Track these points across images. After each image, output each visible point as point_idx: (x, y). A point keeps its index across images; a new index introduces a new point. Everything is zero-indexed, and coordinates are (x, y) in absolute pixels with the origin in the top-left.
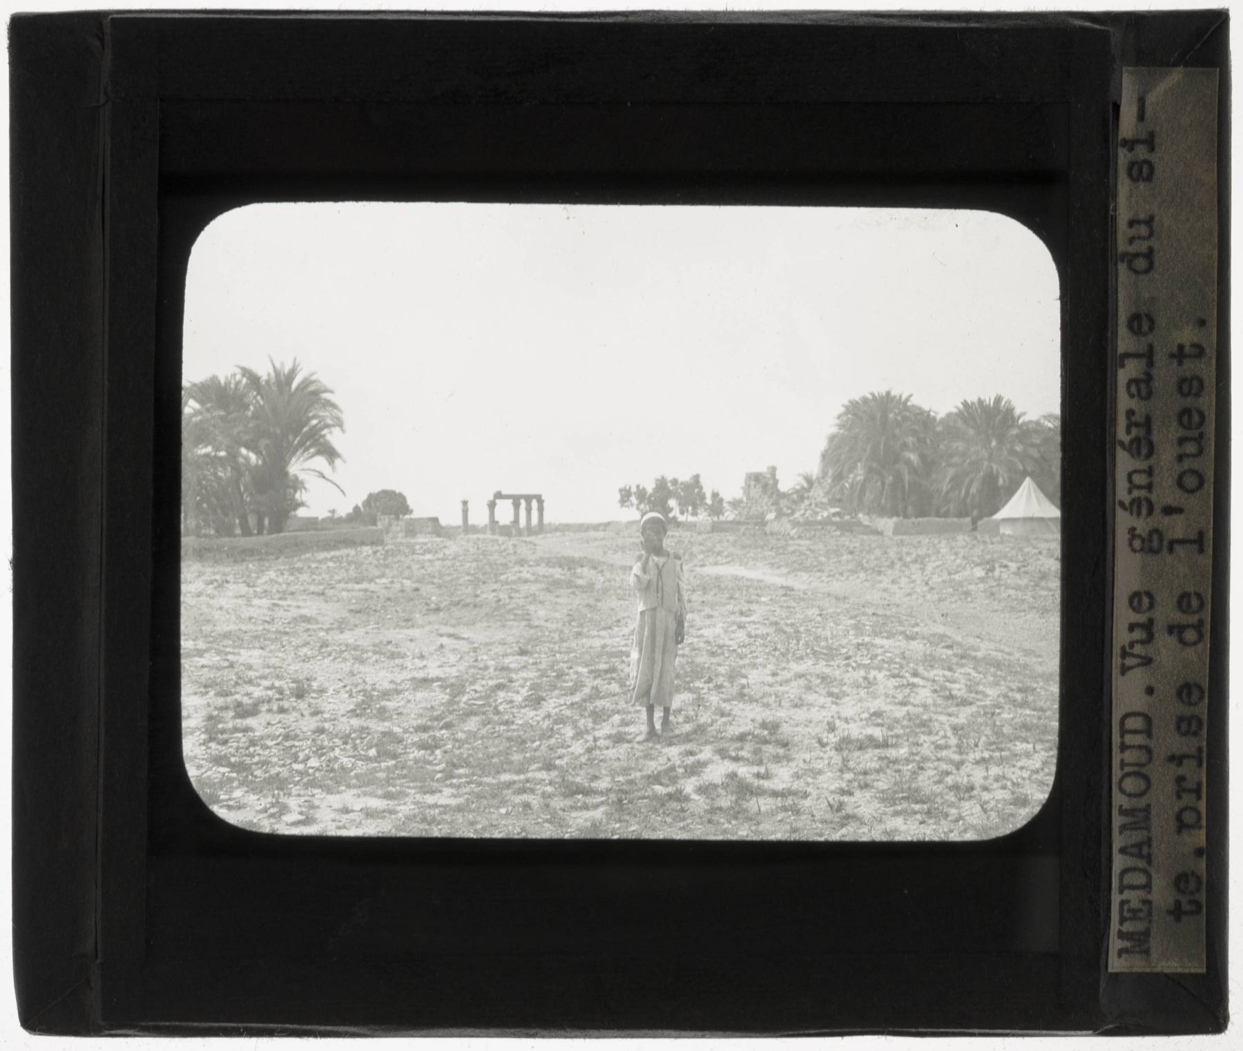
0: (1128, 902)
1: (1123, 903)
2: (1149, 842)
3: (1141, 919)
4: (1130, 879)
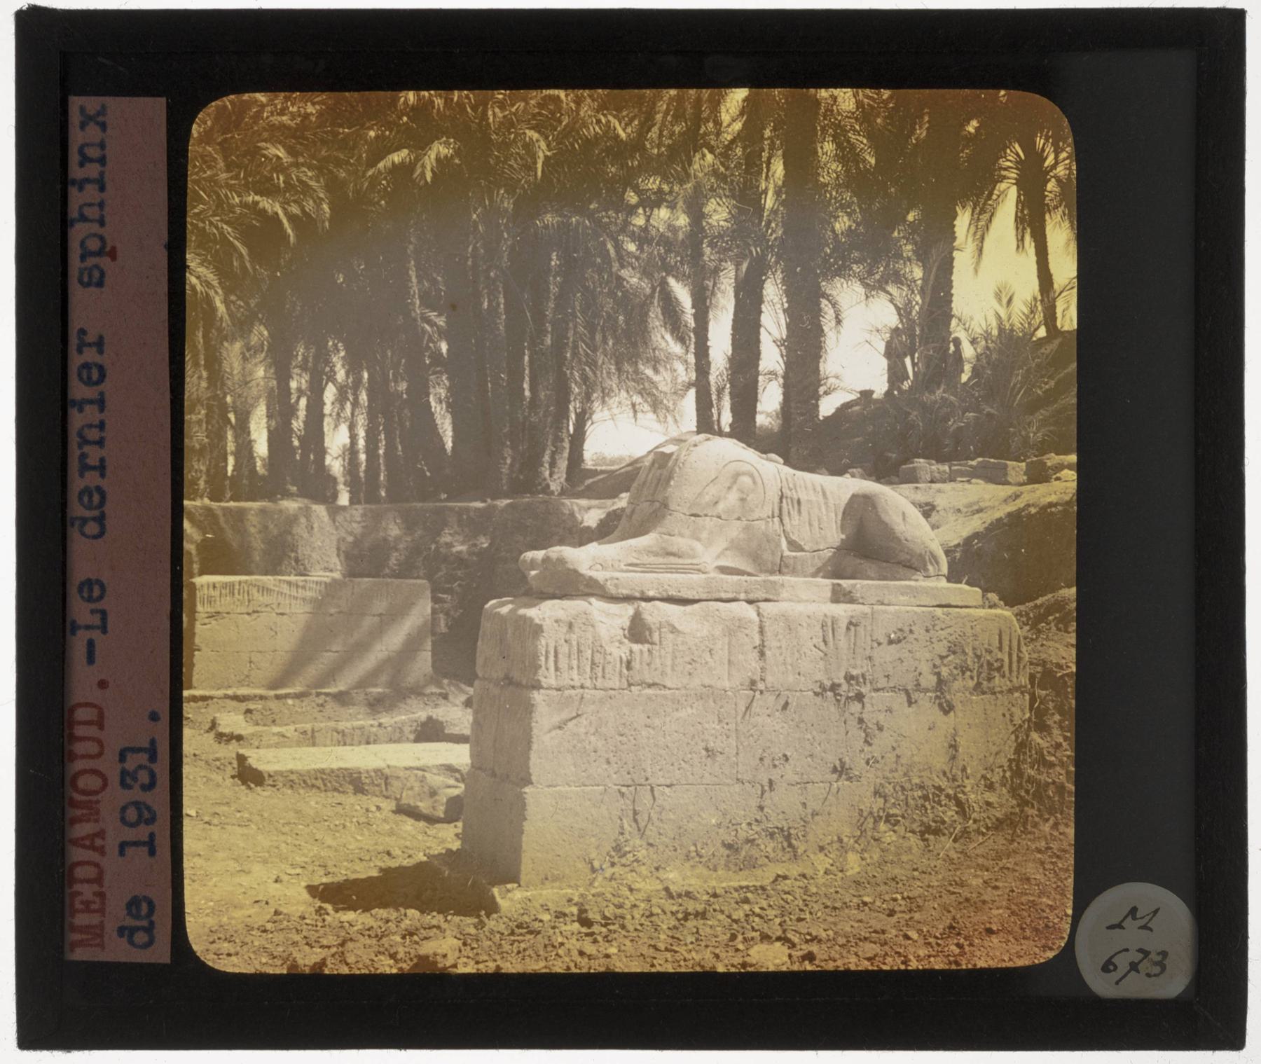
0: (79, 893)
3: (95, 911)
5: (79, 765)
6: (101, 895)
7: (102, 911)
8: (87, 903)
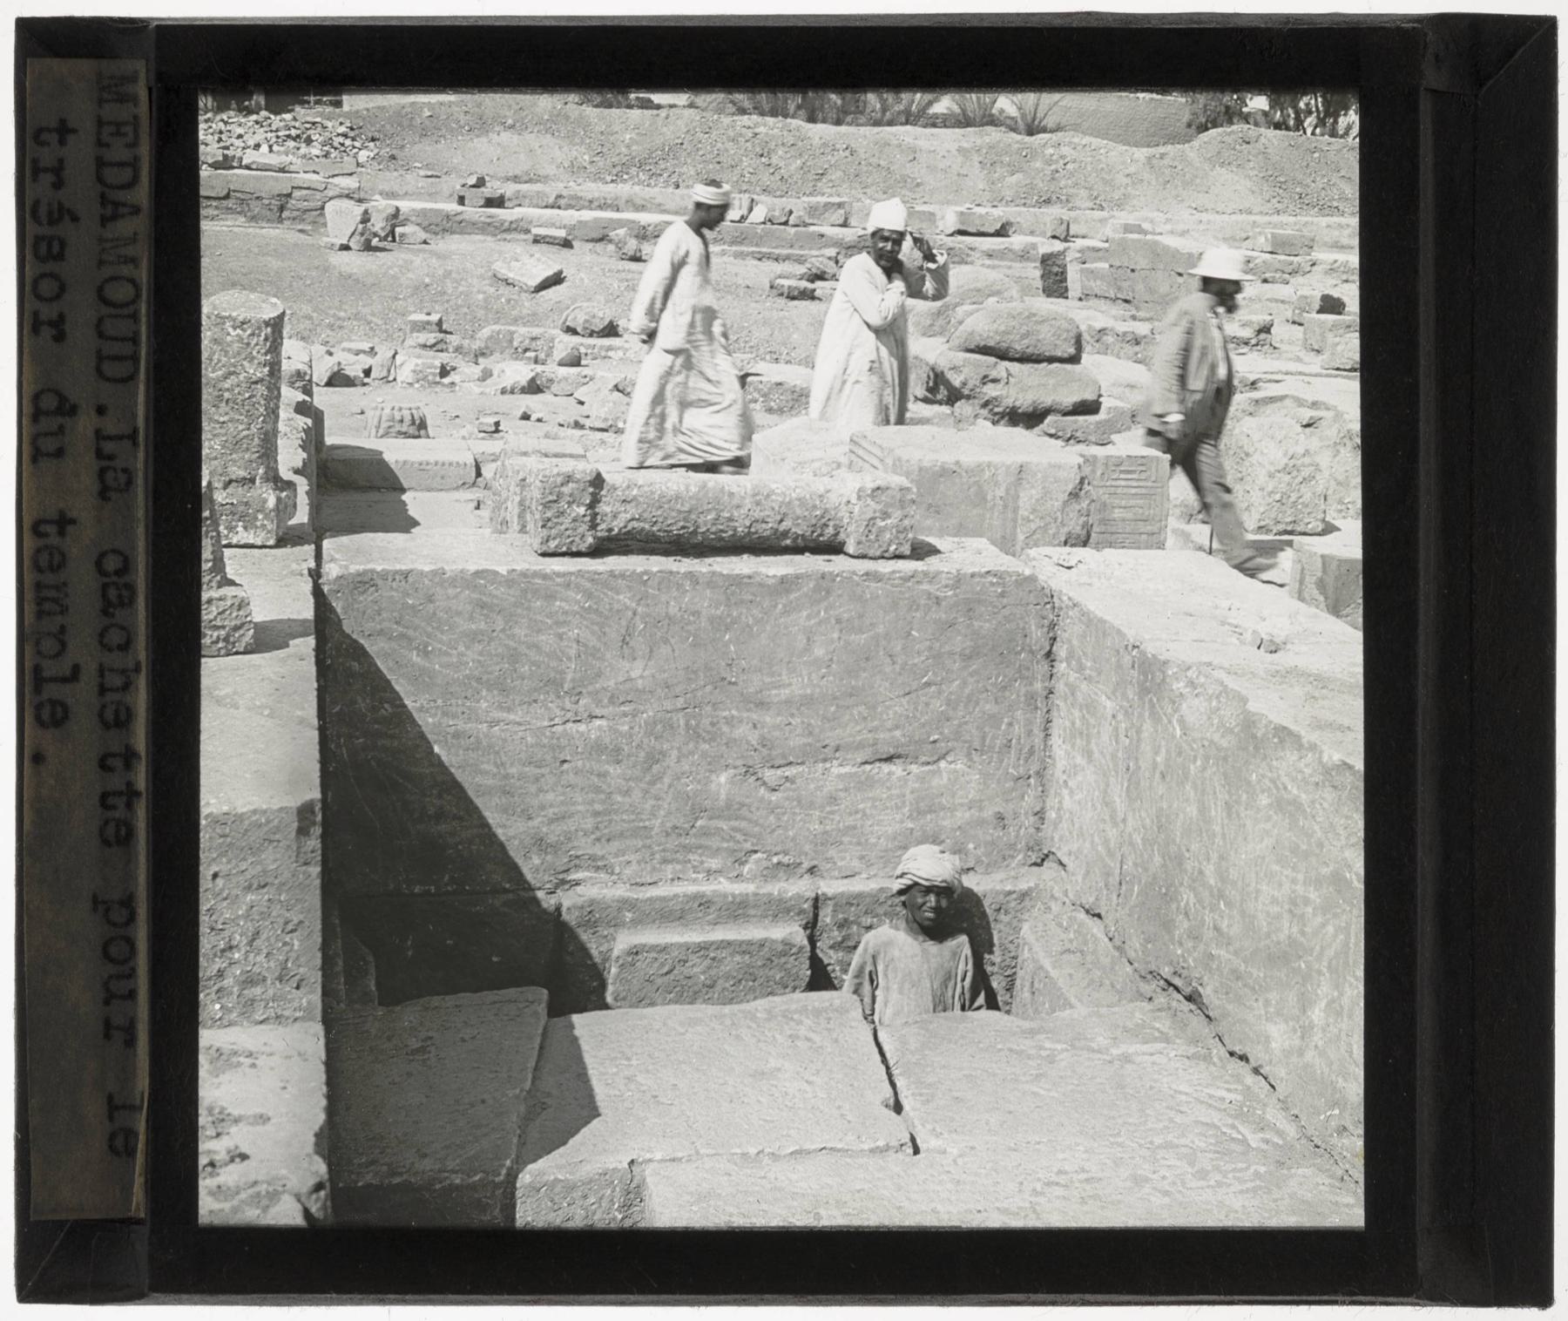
0: (129, 146)
1: (134, 144)
2: (104, 221)
4: (127, 174)
5: (125, 311)
6: (100, 143)
7: (100, 123)
8: (118, 134)
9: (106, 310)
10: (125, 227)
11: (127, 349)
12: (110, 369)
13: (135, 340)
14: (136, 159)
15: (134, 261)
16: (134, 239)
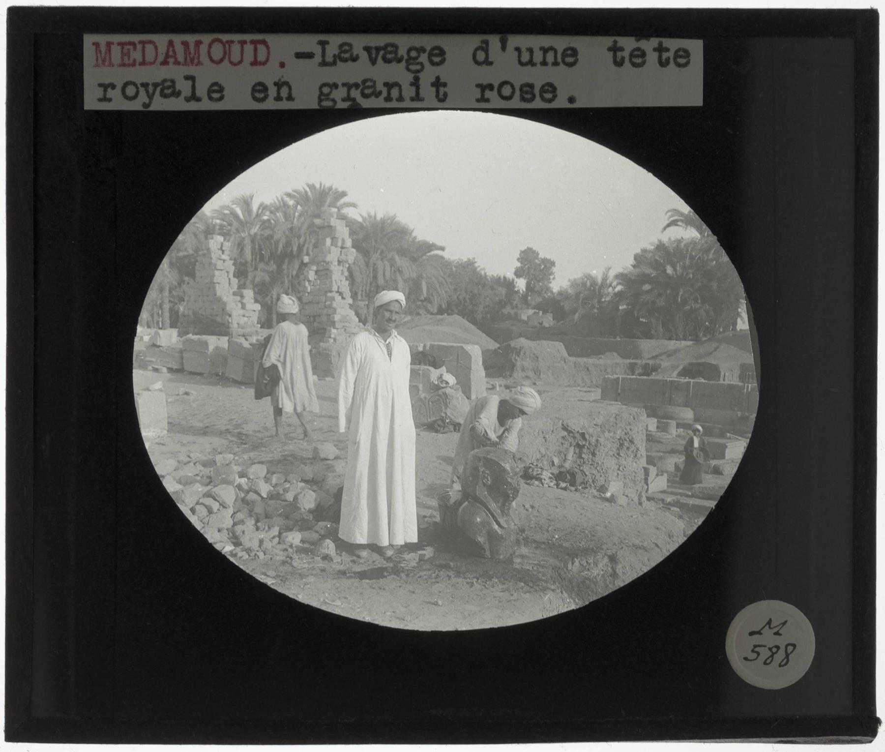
0: (135, 49)
1: (133, 44)
3: (122, 58)
4: (149, 48)
6: (134, 65)
7: (123, 65)
9: (226, 61)
10: (179, 49)
11: (249, 48)
12: (261, 57)
13: (242, 43)
14: (143, 43)
15: (198, 43)
16: (185, 44)
